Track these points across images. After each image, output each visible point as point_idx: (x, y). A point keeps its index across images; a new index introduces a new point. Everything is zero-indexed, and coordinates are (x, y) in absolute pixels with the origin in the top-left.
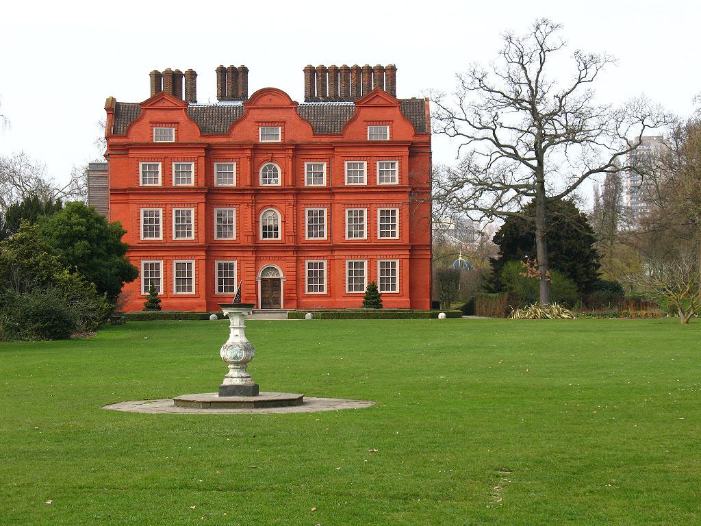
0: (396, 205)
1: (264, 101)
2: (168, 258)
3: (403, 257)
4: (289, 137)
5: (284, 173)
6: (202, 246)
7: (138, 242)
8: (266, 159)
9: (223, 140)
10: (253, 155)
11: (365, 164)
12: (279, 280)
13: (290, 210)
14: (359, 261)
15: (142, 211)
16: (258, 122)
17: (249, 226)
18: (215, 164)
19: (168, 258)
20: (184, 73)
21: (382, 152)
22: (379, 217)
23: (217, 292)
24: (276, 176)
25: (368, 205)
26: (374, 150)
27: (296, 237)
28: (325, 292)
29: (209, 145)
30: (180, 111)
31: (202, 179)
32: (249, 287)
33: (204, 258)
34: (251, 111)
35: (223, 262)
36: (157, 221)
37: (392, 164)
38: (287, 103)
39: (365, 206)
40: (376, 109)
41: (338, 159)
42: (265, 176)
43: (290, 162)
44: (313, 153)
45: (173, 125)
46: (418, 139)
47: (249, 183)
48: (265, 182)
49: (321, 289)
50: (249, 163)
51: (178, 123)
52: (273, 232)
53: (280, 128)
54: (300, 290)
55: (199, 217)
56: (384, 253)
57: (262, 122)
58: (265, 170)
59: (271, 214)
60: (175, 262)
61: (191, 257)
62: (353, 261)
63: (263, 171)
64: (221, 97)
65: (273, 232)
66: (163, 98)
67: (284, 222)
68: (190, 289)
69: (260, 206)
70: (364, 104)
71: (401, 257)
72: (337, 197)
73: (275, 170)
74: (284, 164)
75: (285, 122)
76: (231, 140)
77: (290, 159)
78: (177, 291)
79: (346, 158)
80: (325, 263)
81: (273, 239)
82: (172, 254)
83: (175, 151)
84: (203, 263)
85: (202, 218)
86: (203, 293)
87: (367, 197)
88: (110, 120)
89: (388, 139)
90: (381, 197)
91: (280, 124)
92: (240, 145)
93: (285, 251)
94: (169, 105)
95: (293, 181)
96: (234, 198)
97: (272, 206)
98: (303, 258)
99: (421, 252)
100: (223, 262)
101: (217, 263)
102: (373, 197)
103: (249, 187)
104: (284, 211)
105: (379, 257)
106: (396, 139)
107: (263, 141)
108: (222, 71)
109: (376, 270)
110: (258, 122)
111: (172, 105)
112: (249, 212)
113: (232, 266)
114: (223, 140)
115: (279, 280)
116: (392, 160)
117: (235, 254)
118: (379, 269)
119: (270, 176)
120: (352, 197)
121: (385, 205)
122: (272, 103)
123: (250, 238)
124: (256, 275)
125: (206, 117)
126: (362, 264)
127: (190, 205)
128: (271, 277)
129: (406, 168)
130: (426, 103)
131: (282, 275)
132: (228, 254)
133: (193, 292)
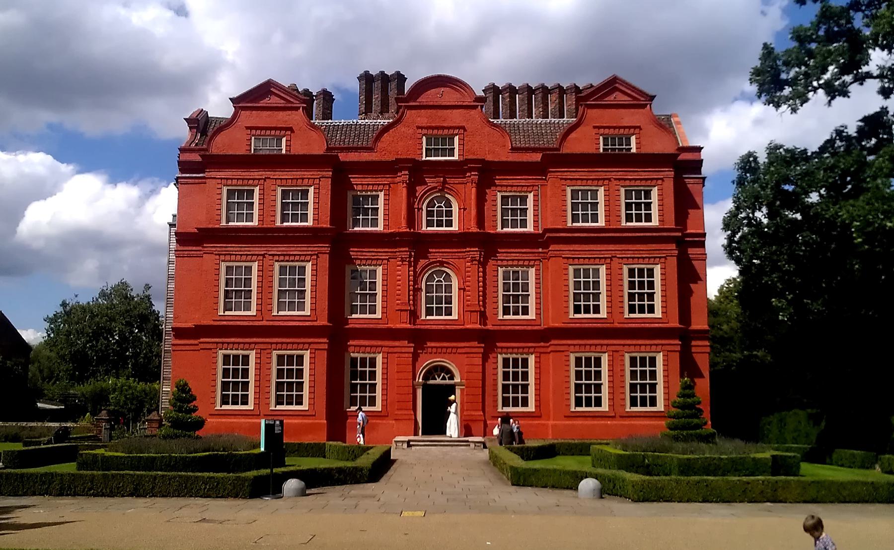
0: (655, 260)
1: (431, 96)
3: (673, 348)
5: (463, 209)
9: (365, 157)
15: (223, 266)
16: (422, 128)
20: (314, 94)
22: (626, 279)
24: (449, 213)
25: (608, 260)
27: (483, 316)
34: (408, 113)
36: (248, 281)
38: (468, 101)
39: (602, 260)
42: (430, 214)
43: (474, 190)
45: (283, 132)
46: (684, 156)
48: (430, 224)
49: (525, 402)
51: (291, 129)
52: (444, 305)
60: (275, 353)
62: (583, 355)
63: (428, 207)
65: (444, 305)
69: (422, 262)
73: (449, 204)
75: (463, 128)
81: (444, 317)
91: (456, 131)
94: (281, 103)
97: (442, 264)
106: (644, 150)
107: (428, 158)
109: (623, 370)
110: (422, 128)
112: (403, 272)
118: (628, 369)
119: (440, 214)
123: (406, 316)
124: (414, 378)
128: (439, 381)
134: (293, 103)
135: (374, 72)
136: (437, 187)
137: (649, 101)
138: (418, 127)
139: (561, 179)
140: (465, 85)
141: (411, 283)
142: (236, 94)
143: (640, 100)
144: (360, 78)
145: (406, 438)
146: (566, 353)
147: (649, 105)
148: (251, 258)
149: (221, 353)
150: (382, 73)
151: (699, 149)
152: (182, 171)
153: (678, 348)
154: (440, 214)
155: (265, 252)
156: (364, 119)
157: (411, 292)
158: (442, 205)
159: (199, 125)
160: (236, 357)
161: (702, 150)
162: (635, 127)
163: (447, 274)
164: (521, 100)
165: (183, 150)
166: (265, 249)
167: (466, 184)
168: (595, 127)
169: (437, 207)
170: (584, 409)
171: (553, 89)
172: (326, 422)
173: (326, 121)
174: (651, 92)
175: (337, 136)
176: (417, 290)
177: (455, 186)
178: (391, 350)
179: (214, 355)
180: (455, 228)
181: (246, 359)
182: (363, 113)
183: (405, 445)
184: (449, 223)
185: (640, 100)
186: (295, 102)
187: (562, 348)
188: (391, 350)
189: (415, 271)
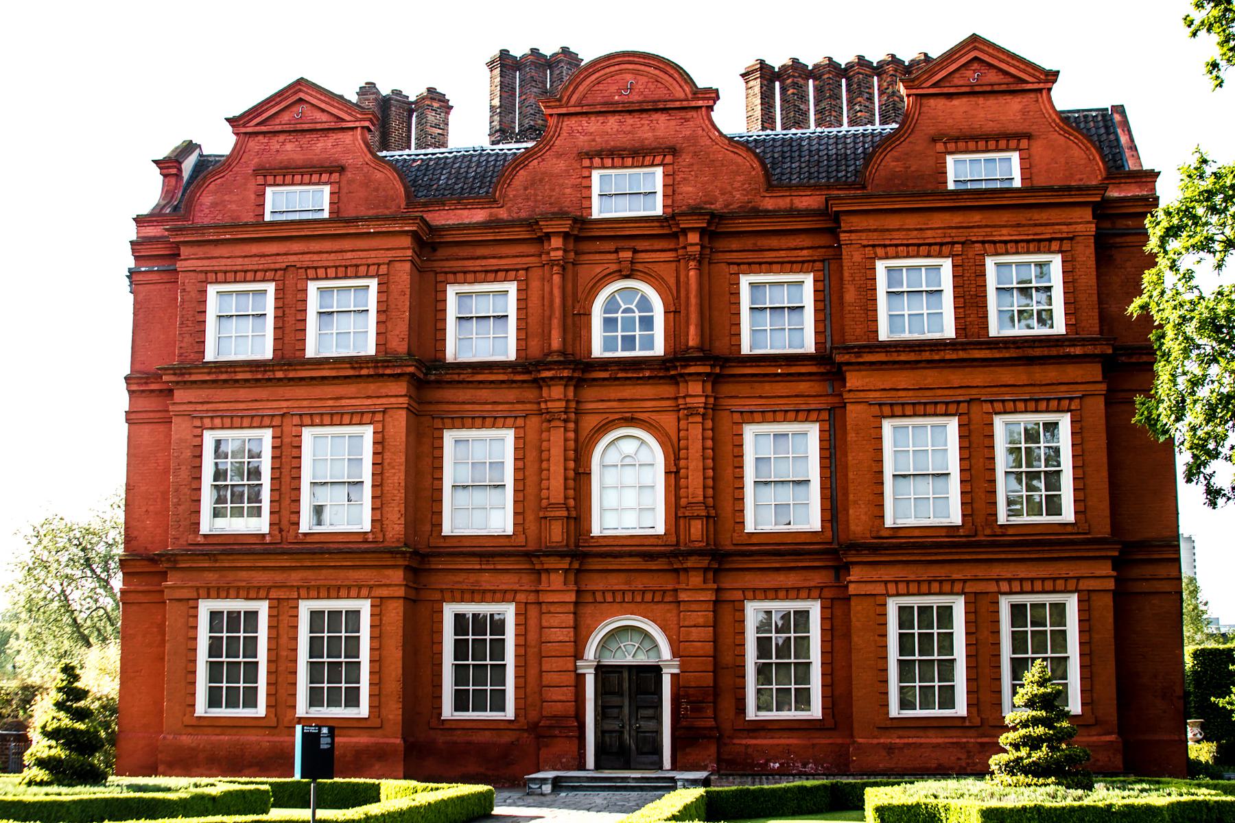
2: (281, 594)
4: (690, 192)
5: (673, 312)
6: (392, 552)
7: (191, 538)
8: (613, 267)
10: (572, 255)
11: (947, 265)
12: (656, 670)
13: (695, 432)
14: (934, 601)
15: (209, 438)
17: (556, 486)
18: (451, 291)
19: (281, 594)
21: (1003, 225)
23: (448, 711)
24: (647, 323)
26: (976, 218)
28: (816, 711)
29: (432, 230)
30: (347, 138)
31: (401, 328)
32: (556, 694)
33: (401, 592)
35: (469, 609)
37: (1040, 265)
40: (973, 100)
41: (852, 257)
42: (609, 323)
44: (774, 242)
45: (325, 177)
47: (556, 343)
48: (609, 344)
49: (803, 699)
50: (557, 279)
51: (342, 169)
53: (659, 171)
54: (727, 704)
55: (387, 455)
56: (1022, 571)
57: (600, 154)
58: (611, 306)
59: (628, 447)
61: (354, 591)
62: (915, 601)
64: (502, 133)
66: (301, 100)
67: (674, 473)
68: (353, 699)
69: (590, 422)
70: (935, 85)
71: (1084, 585)
72: (854, 380)
73: (645, 304)
74: (672, 281)
75: (674, 151)
76: (503, 214)
77: (692, 264)
78: (311, 704)
79: (880, 251)
80: (815, 610)
82: (295, 578)
83: (315, 246)
84: (395, 612)
85: (397, 458)
86: (394, 712)
87: (957, 377)
88: (168, 193)
89: (1017, 183)
90: (1006, 375)
91: (658, 159)
92: (531, 224)
93: (677, 571)
95: (702, 335)
96: (511, 394)
97: (631, 421)
98: (738, 595)
99: (1148, 570)
100: (469, 609)
101: (449, 611)
102: (979, 377)
103: (555, 358)
104: (675, 439)
105: (1004, 586)
106: (1040, 181)
108: (505, 63)
111: (324, 117)
112: (557, 440)
113: (499, 627)
114: (479, 216)
115: (656, 670)
116: (1039, 251)
117: (508, 581)
119: (628, 323)
120: (903, 379)
121: (1021, 406)
122: (636, 98)
124: (578, 655)
125: (448, 179)
126: (946, 614)
127: (356, 417)
128: (629, 660)
129: (1088, 279)
130: (1117, 117)
131: (666, 652)
132: (487, 581)
133: (363, 710)
134: (343, 120)
135: (518, 51)
136: (620, 271)
137: (1046, 82)
138: (582, 155)
139: (865, 246)
140: (677, 68)
141: (572, 464)
142: (237, 111)
143: (1027, 82)
144: (491, 65)
145: (551, 774)
146: (879, 600)
147: (1044, 92)
148: (257, 421)
149: (205, 607)
150: (534, 51)
151: (1154, 175)
152: (137, 258)
153: (1111, 584)
154: (628, 323)
155: (285, 410)
156: (498, 143)
157: (571, 483)
158: (633, 307)
159: (180, 170)
160: (233, 617)
161: (1159, 179)
162: (1018, 136)
163: (643, 442)
164: (818, 90)
165: (139, 220)
166: (285, 404)
167: (679, 261)
168: (934, 140)
169: (623, 312)
170: (919, 713)
171: (882, 67)
172: (399, 741)
173: (423, 151)
174: (1047, 66)
175: (439, 179)
176: (580, 477)
177: (656, 267)
178: (532, 598)
179: (192, 612)
180: (659, 349)
181: (252, 616)
182: (496, 132)
183: (547, 788)
184: (649, 343)
185: (1027, 82)
186: (347, 118)
187: (869, 589)
188: (532, 598)
189: (576, 440)
